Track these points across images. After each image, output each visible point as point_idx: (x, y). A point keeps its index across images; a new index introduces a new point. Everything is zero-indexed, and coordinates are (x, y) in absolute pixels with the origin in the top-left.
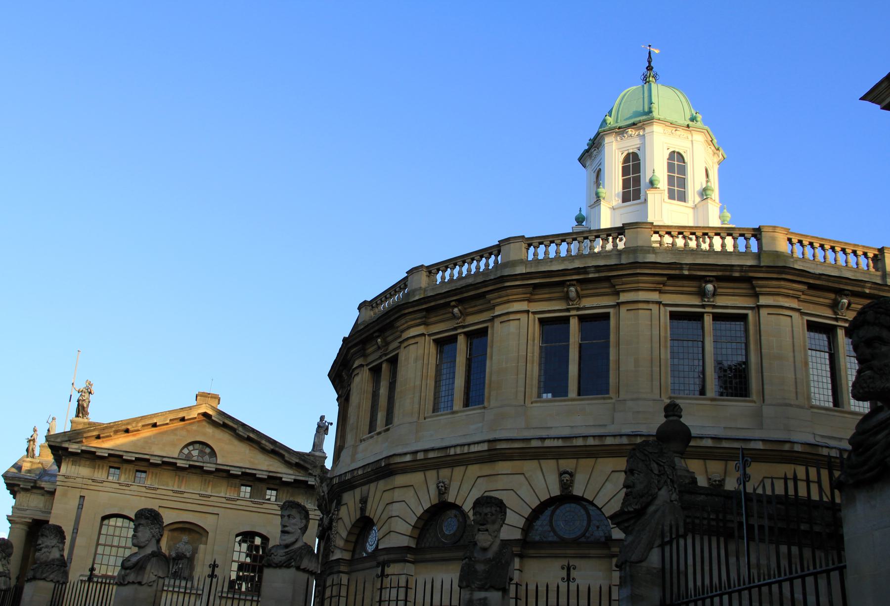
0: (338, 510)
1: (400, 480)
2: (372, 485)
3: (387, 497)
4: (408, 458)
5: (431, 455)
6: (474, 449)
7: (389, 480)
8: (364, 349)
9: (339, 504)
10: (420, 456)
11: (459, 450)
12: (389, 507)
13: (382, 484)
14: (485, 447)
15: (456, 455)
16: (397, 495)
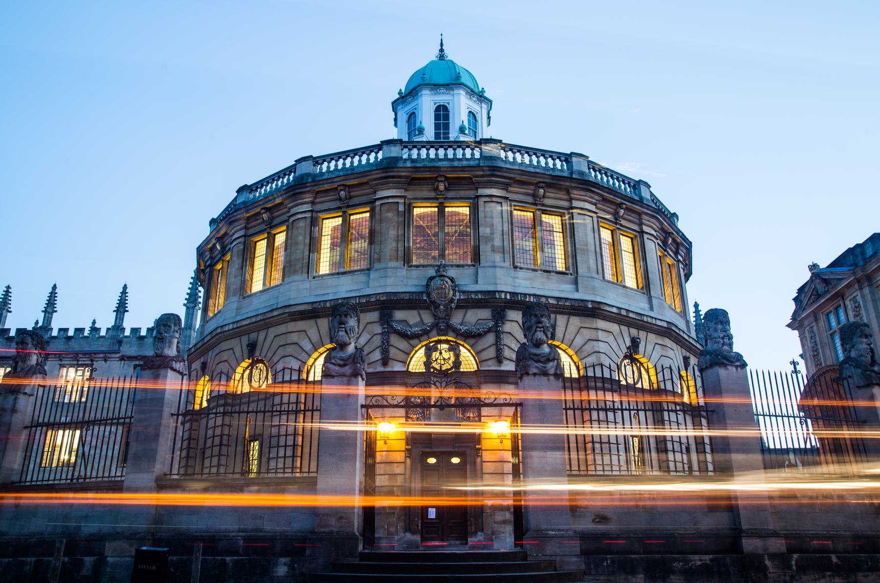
0: (503, 323)
1: (601, 324)
2: (559, 317)
3: (587, 334)
4: (614, 310)
5: (631, 315)
6: (659, 323)
7: (590, 319)
8: (509, 185)
9: (499, 317)
10: (624, 313)
11: (650, 320)
12: (595, 343)
13: (575, 321)
14: (665, 325)
15: (647, 322)
16: (601, 335)
